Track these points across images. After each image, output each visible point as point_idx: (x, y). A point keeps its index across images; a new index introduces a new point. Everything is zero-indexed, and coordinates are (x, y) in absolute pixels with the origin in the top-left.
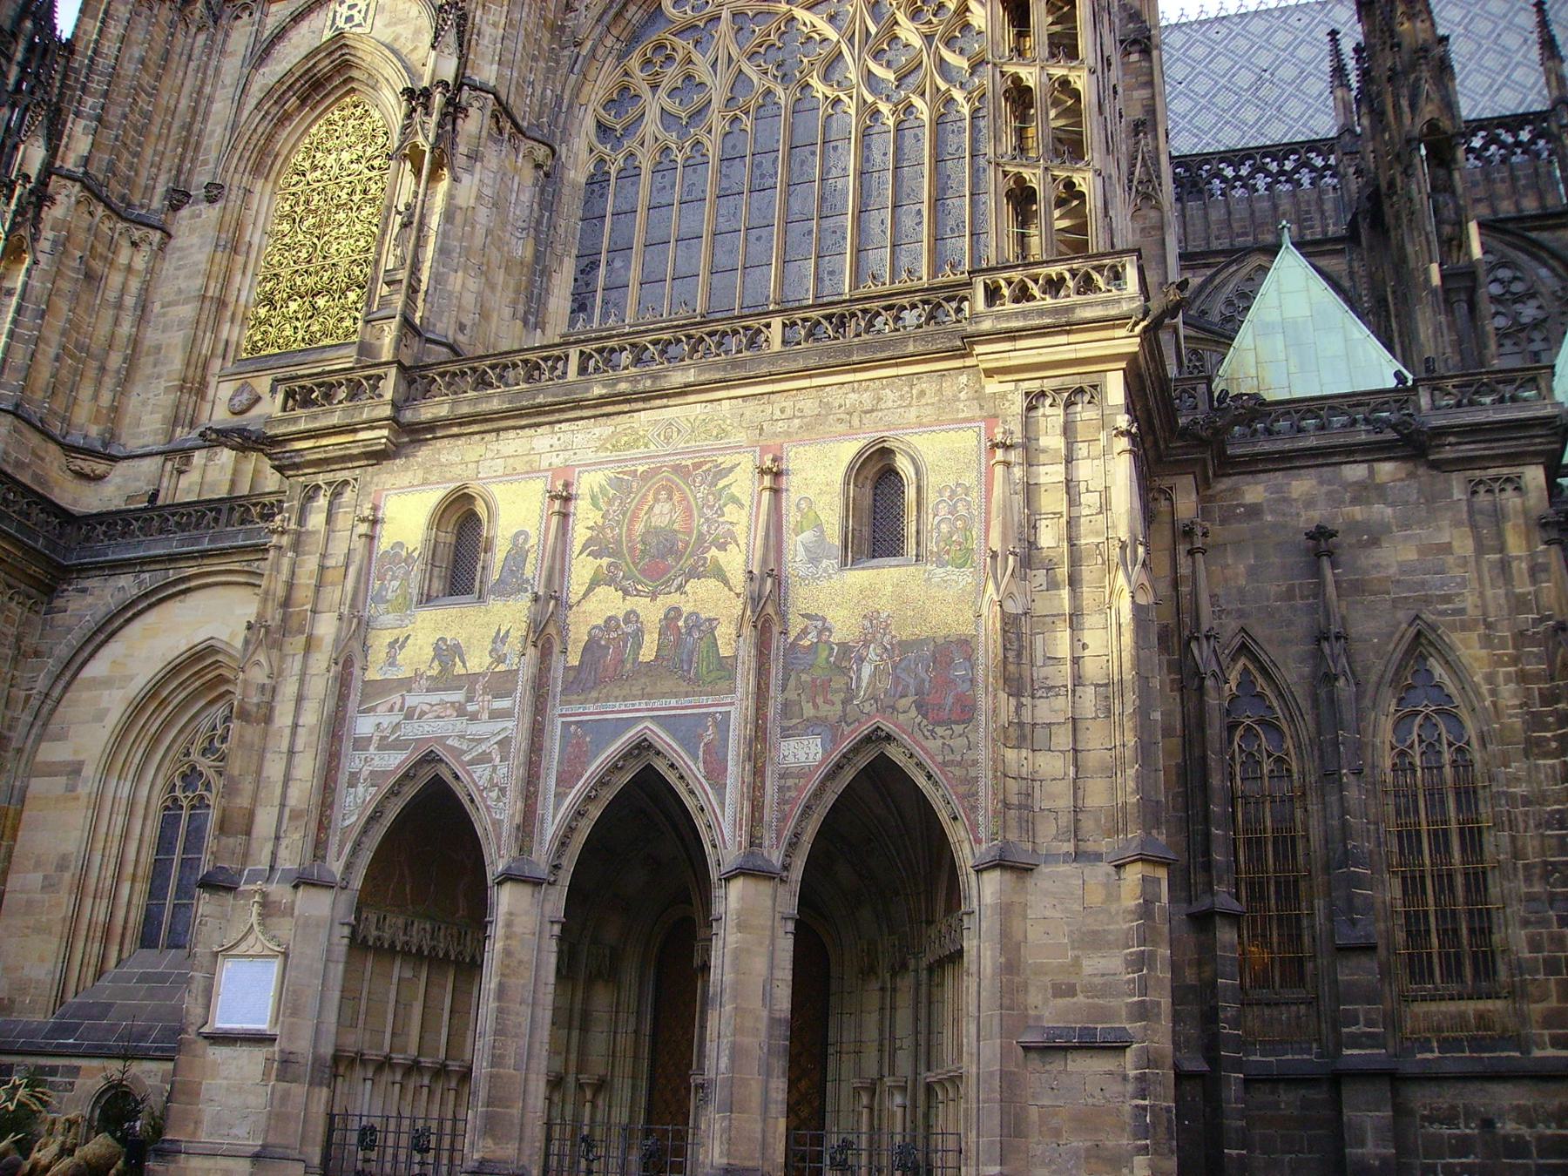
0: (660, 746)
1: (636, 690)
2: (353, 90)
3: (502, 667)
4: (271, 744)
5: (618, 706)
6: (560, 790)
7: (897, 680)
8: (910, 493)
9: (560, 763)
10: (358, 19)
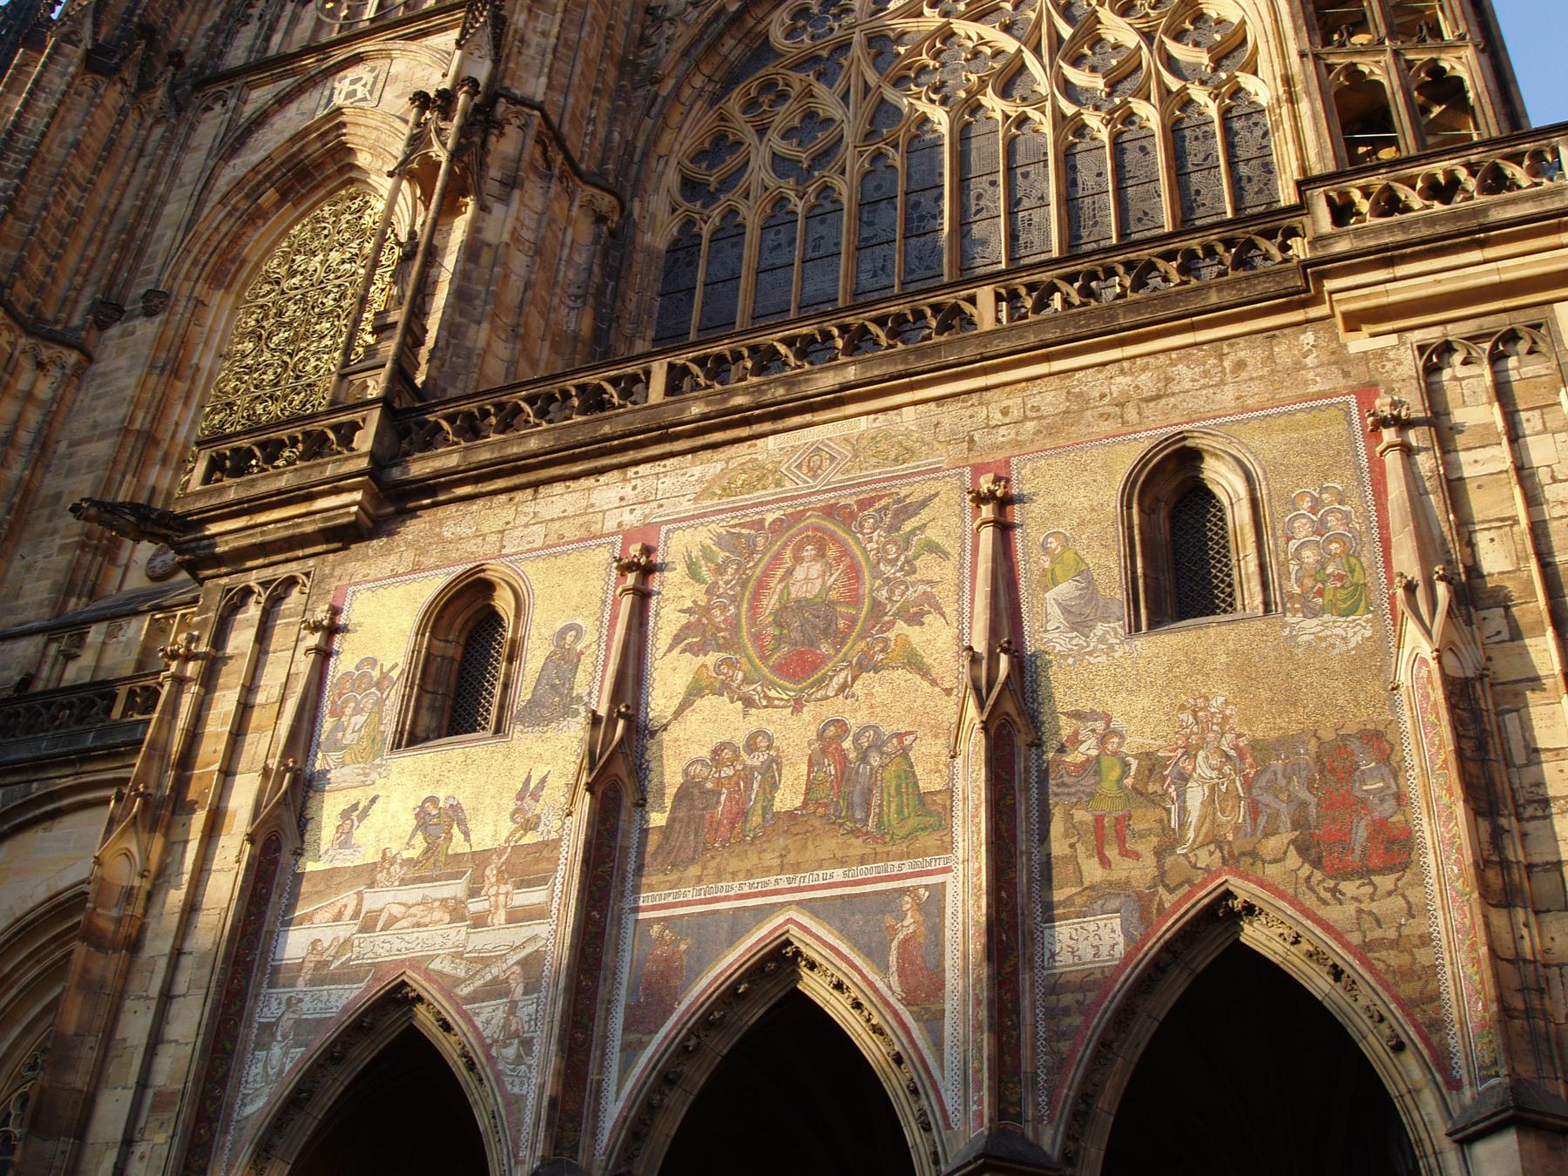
1: (771, 859)
2: (352, 181)
3: (530, 838)
4: (135, 986)
5: (736, 887)
6: (632, 1037)
7: (1254, 809)
8: (1239, 516)
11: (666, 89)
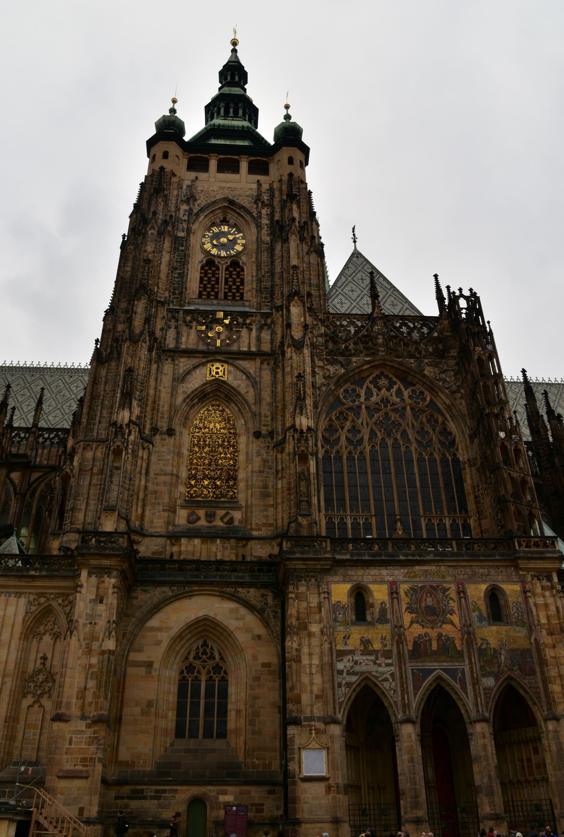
0: (444, 678)
8: (502, 602)
9: (413, 681)
10: (221, 374)
11: (319, 410)
